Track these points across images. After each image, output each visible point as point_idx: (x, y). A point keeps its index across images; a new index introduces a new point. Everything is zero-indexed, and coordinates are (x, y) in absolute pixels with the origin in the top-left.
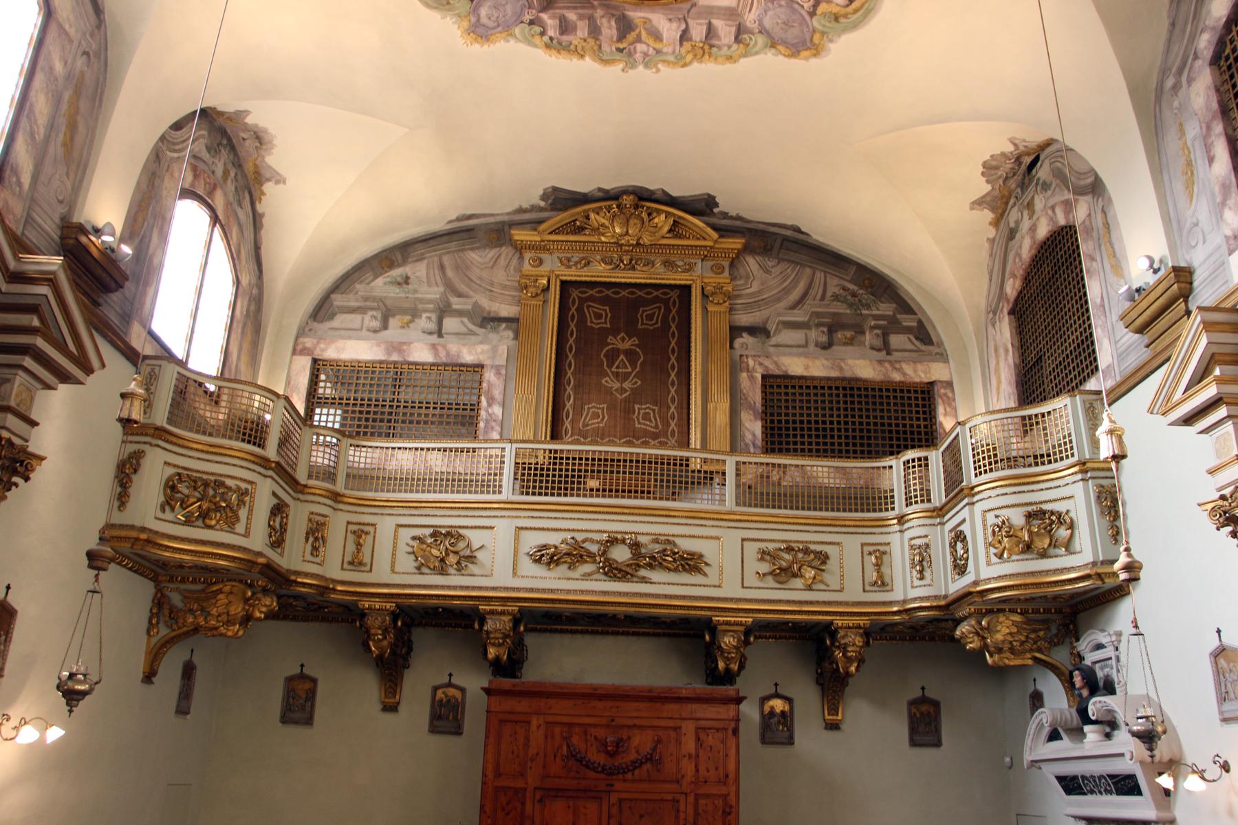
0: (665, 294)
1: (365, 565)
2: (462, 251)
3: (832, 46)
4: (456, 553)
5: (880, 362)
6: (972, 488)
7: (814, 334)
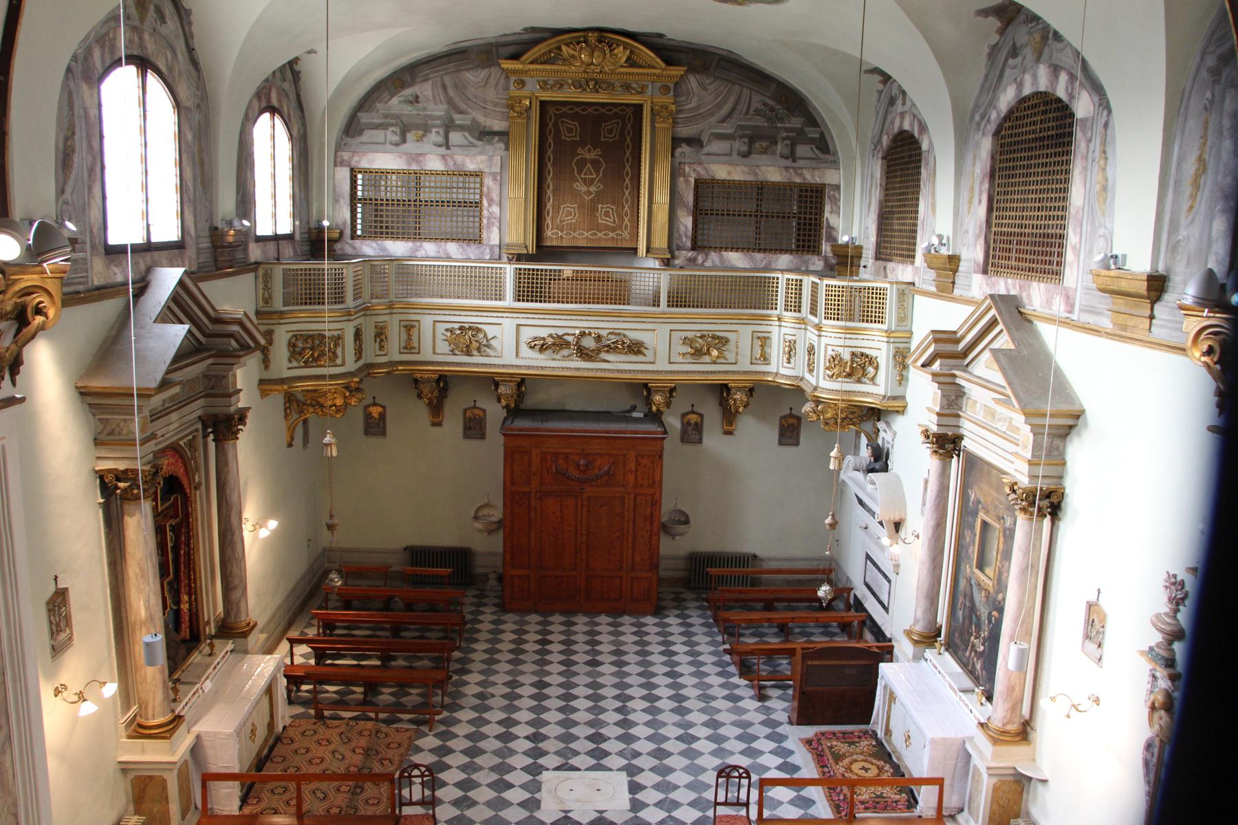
0: (622, 110)
2: (459, 71)
5: (787, 168)
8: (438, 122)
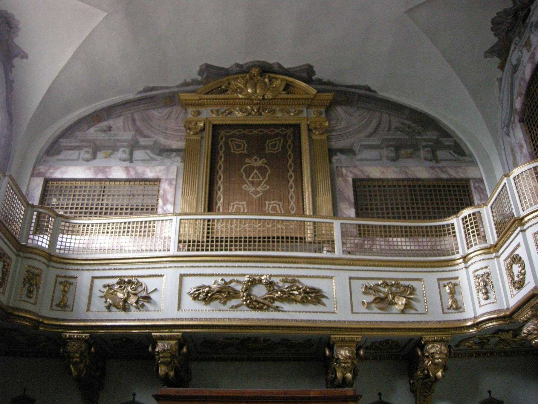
1: (68, 307)
4: (135, 295)
5: (432, 168)
6: (523, 219)
7: (385, 152)
8: (126, 144)
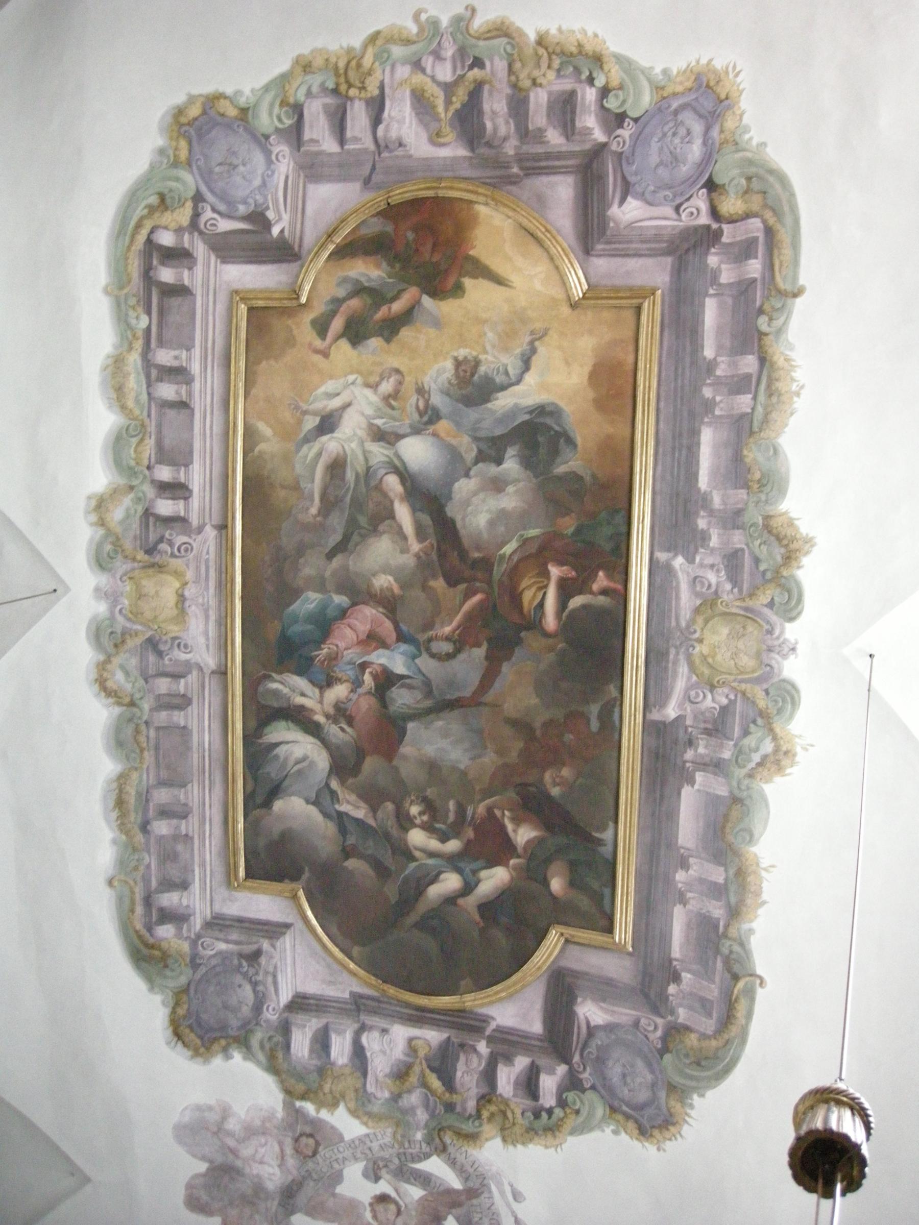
3: (160, 142)
